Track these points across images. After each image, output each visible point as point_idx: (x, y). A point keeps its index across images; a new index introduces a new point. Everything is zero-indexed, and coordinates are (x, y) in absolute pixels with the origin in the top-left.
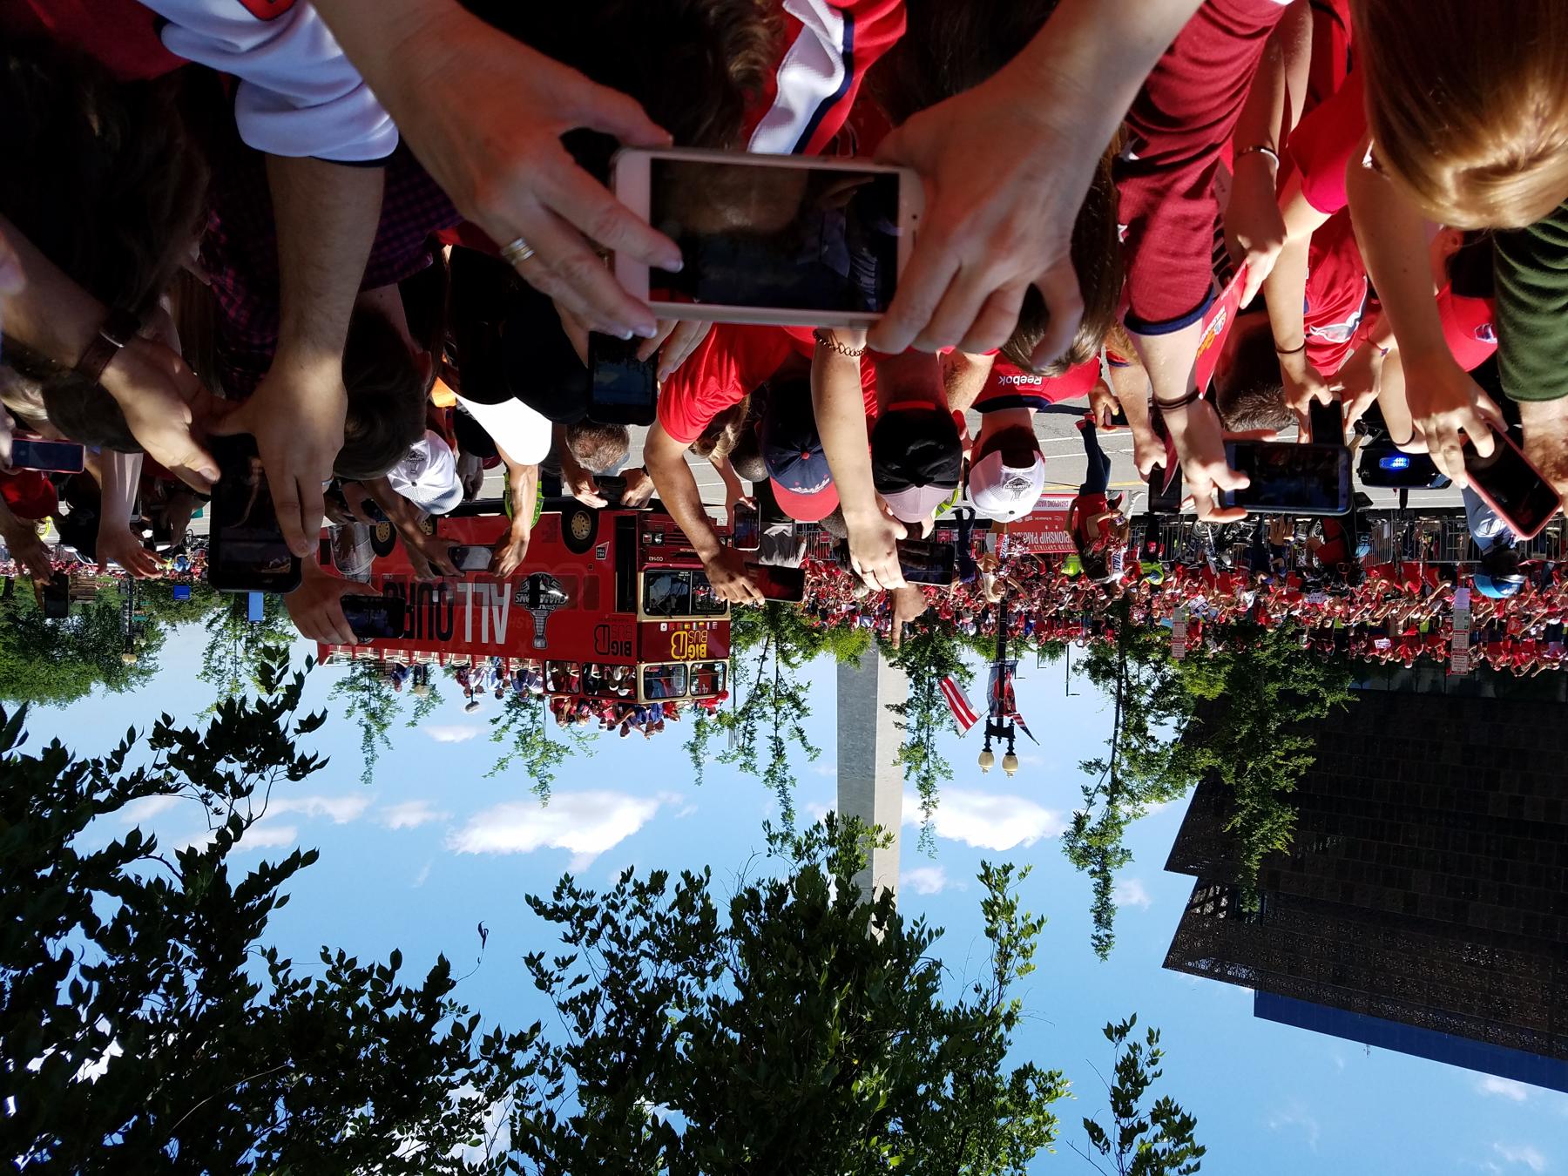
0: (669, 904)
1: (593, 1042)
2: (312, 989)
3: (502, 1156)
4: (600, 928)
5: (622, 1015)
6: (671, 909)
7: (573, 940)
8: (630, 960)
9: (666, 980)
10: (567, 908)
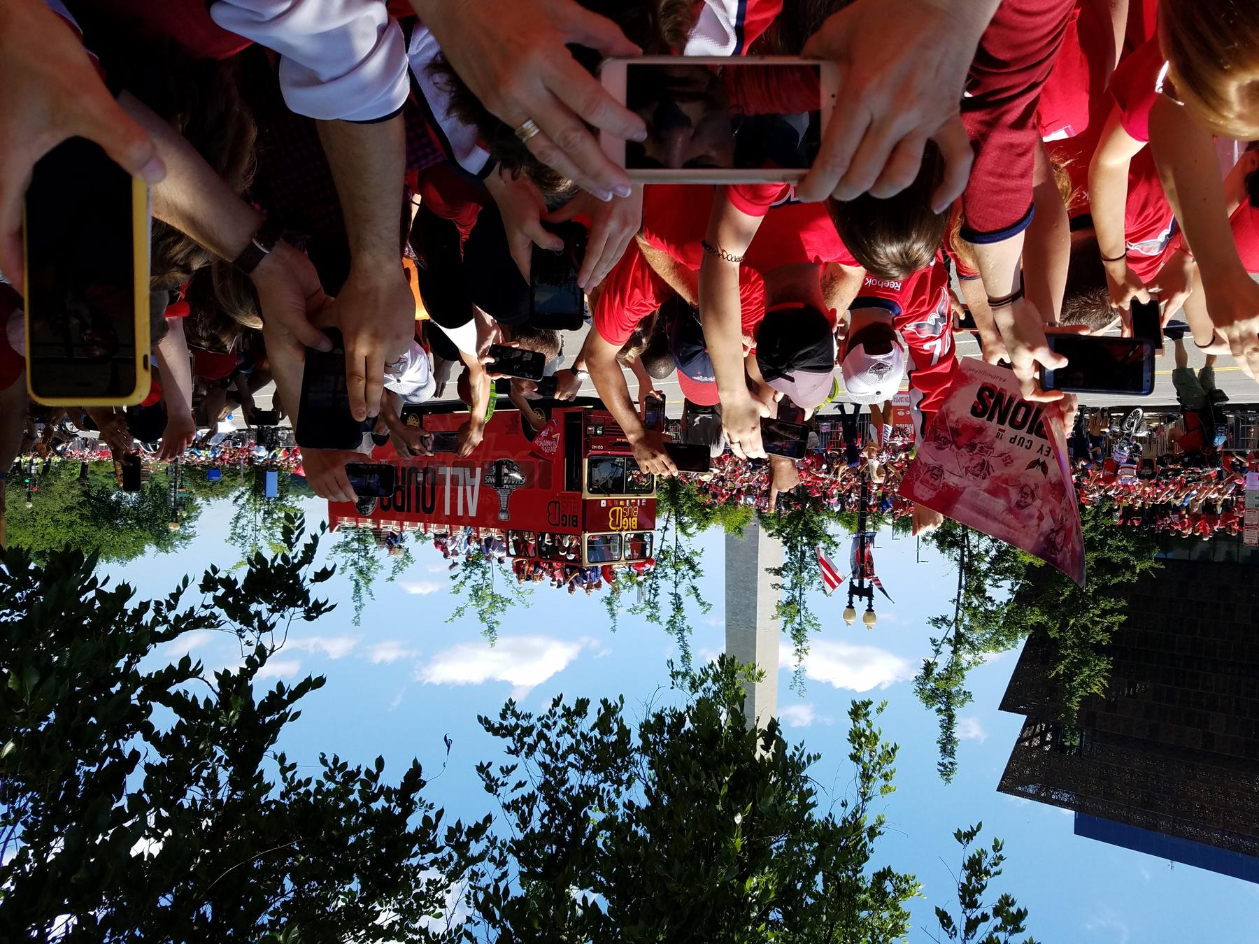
1: (531, 836)
2: (312, 787)
3: (459, 927)
4: (536, 744)
5: (554, 814)
6: (592, 730)
7: (515, 752)
8: (560, 769)
10: (511, 726)
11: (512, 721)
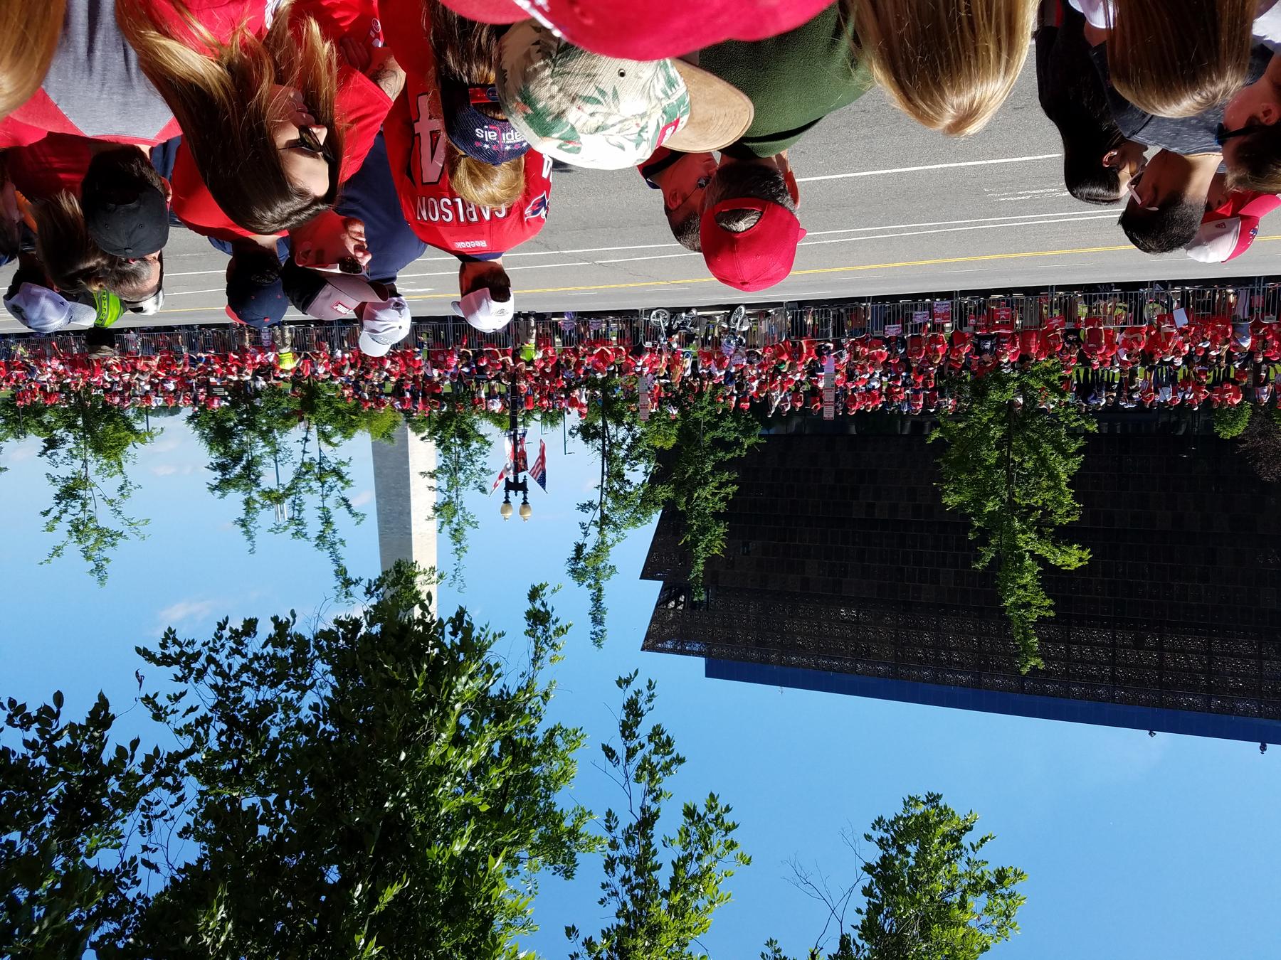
0: (262, 643)
4: (205, 669)
6: (265, 646)
7: (184, 679)
8: (234, 690)
9: (266, 702)
11: (173, 650)
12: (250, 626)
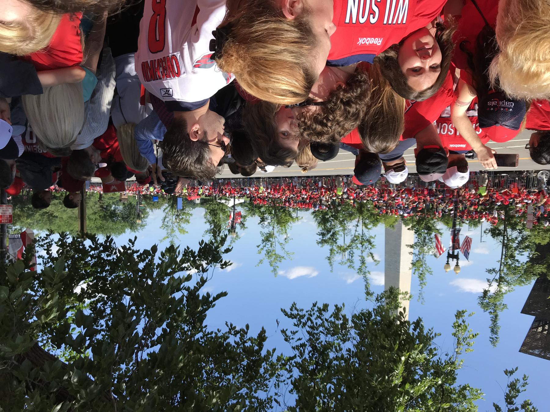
0: (330, 315)
2: (213, 335)
3: (271, 397)
6: (331, 317)
8: (316, 334)
10: (293, 314)
12: (326, 307)
